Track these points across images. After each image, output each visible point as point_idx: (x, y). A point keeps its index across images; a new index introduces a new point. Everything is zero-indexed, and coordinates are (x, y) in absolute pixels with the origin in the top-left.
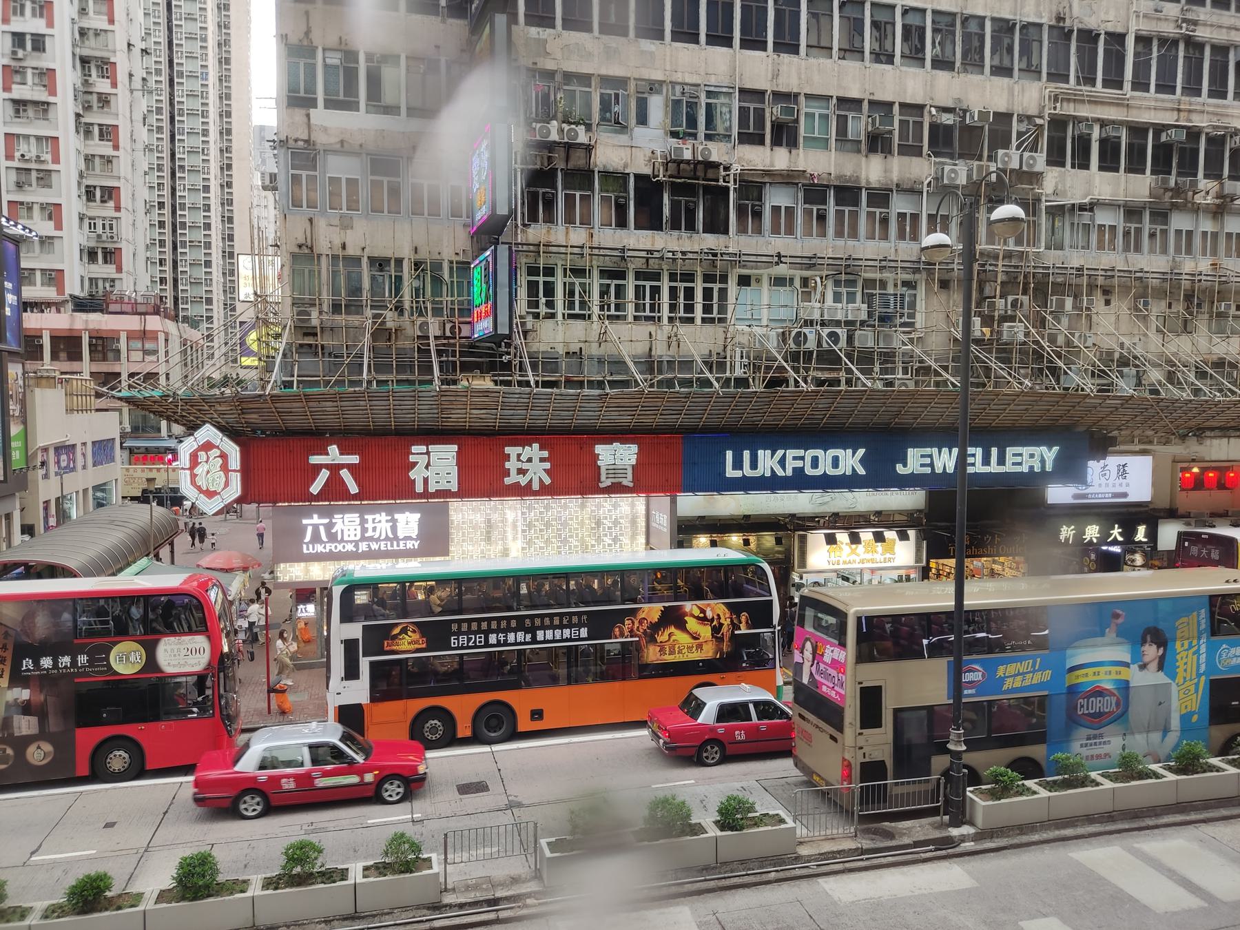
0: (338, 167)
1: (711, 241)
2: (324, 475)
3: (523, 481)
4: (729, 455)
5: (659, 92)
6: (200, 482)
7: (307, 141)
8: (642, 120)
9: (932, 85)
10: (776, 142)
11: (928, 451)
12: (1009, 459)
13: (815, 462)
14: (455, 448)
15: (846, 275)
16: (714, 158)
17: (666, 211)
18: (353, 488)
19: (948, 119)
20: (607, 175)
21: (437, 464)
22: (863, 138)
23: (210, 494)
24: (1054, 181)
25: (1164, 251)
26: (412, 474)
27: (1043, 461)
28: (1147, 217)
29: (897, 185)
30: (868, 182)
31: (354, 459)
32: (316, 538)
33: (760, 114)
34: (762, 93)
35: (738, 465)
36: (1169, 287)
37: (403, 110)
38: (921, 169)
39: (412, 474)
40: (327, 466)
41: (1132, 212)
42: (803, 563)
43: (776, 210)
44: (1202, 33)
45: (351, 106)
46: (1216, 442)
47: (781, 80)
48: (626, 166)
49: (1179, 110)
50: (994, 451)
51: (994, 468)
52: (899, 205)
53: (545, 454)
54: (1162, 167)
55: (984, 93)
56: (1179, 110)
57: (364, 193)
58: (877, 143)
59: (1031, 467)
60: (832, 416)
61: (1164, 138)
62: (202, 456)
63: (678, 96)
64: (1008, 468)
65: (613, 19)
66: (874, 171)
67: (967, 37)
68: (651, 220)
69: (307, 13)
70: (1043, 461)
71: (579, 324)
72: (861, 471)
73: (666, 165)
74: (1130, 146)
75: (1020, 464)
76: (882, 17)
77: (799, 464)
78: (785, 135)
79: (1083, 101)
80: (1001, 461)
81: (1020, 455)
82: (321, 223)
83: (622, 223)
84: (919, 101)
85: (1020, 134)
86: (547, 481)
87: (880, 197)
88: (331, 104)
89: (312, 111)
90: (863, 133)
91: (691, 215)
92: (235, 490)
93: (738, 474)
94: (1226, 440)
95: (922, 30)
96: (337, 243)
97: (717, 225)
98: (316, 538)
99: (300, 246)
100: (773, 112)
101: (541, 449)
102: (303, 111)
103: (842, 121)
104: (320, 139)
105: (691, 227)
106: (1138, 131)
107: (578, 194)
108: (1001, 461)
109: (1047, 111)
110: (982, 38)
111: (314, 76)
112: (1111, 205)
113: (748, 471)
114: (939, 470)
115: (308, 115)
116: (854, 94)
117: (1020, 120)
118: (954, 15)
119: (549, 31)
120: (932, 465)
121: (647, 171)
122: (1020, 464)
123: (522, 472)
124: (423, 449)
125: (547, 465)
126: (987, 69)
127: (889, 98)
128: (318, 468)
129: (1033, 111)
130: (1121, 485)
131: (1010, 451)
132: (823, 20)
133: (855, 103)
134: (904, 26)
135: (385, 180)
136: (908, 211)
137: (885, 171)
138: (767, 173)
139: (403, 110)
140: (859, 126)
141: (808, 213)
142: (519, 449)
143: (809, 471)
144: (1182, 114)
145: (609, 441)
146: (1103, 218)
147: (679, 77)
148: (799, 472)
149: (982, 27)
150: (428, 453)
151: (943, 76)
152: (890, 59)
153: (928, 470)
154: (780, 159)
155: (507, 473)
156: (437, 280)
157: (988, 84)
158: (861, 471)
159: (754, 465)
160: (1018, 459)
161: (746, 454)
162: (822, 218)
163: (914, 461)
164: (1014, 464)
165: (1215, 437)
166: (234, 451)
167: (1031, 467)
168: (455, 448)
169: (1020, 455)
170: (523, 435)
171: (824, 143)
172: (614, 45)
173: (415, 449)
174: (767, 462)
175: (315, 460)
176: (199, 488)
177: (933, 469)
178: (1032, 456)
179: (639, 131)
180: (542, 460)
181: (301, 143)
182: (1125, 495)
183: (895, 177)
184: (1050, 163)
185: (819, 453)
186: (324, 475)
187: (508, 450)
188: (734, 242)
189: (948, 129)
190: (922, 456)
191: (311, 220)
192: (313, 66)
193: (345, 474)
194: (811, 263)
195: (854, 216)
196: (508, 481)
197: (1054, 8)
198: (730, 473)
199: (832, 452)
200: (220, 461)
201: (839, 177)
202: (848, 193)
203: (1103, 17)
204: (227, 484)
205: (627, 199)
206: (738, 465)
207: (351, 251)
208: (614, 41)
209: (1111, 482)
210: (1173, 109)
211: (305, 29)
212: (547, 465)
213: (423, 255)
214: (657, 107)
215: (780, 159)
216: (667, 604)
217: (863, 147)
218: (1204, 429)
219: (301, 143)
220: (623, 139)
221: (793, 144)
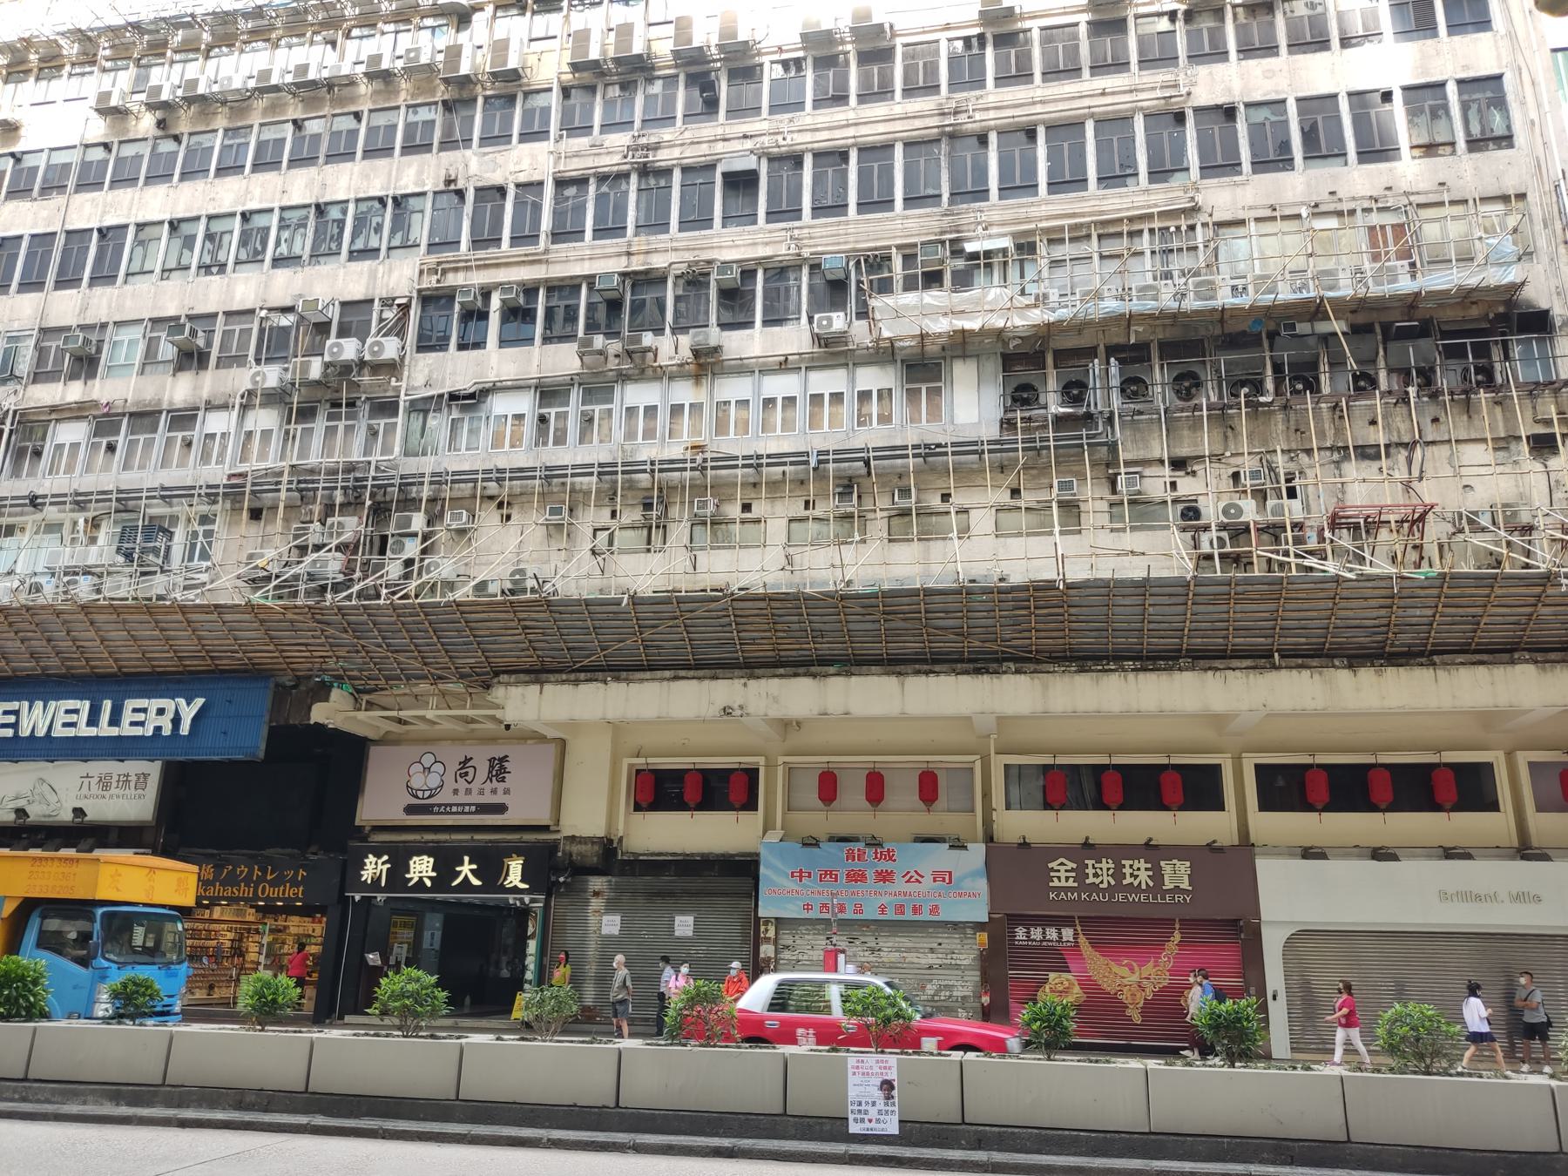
9: (266, 286)
10: (73, 376)
11: (14, 705)
12: (128, 716)
19: (286, 321)
24: (426, 371)
27: (176, 721)
28: (575, 395)
29: (208, 402)
30: (171, 403)
36: (615, 483)
41: (549, 392)
44: (664, 157)
46: (515, 692)
47: (89, 313)
49: (629, 254)
50: (107, 705)
55: (336, 281)
56: (629, 254)
58: (191, 359)
59: (158, 729)
66: (181, 390)
70: (176, 721)
75: (141, 724)
79: (468, 268)
80: (115, 721)
81: (144, 710)
84: (248, 306)
94: (538, 687)
108: (115, 721)
112: (517, 387)
114: (25, 732)
120: (15, 726)
122: (141, 724)
127: (210, 309)
130: (494, 791)
131: (130, 704)
137: (195, 389)
138: (54, 409)
144: (634, 259)
151: (282, 275)
153: (9, 733)
154: (74, 392)
157: (342, 271)
160: (140, 717)
162: (111, 448)
164: (133, 724)
165: (517, 684)
167: (158, 729)
169: (144, 710)
177: (16, 732)
178: (161, 712)
182: (500, 809)
190: (6, 713)
197: (443, 173)
201: (137, 403)
203: (512, 168)
209: (475, 786)
210: (619, 255)
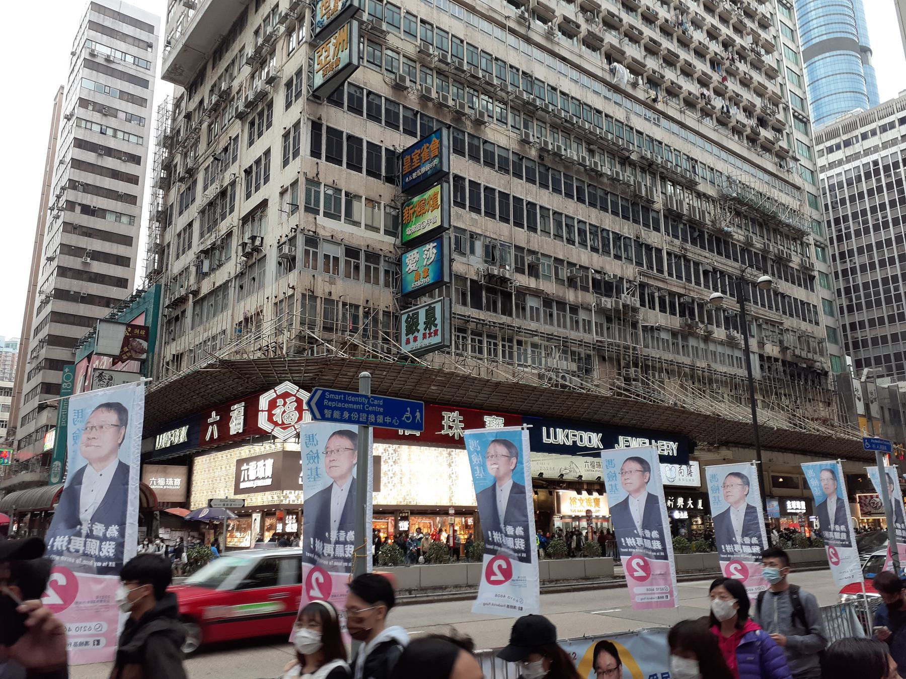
0: (326, 248)
1: (505, 319)
4: (544, 429)
5: (480, 240)
6: (278, 419)
7: (315, 232)
8: (472, 252)
15: (565, 346)
16: (507, 276)
17: (484, 300)
19: (598, 276)
25: (689, 356)
33: (523, 259)
34: (523, 249)
35: (548, 436)
37: (363, 225)
38: (590, 298)
42: (559, 511)
43: (531, 308)
45: (338, 218)
52: (582, 315)
53: (461, 418)
54: (682, 315)
55: (614, 268)
58: (571, 282)
60: (589, 413)
61: (682, 300)
63: (487, 243)
65: (459, 200)
66: (571, 296)
67: (603, 237)
68: (477, 304)
74: (670, 302)
76: (570, 222)
78: (533, 271)
82: (319, 279)
84: (587, 265)
85: (627, 289)
87: (574, 309)
88: (326, 215)
91: (495, 303)
95: (585, 232)
96: (327, 291)
97: (507, 311)
100: (528, 259)
102: (313, 216)
103: (556, 269)
104: (322, 233)
105: (495, 311)
106: (672, 294)
109: (638, 279)
110: (609, 239)
111: (319, 198)
113: (552, 440)
116: (561, 257)
118: (597, 227)
121: (475, 278)
123: (450, 427)
126: (612, 255)
129: (631, 279)
132: (546, 219)
133: (562, 261)
134: (579, 229)
135: (353, 260)
136: (587, 319)
140: (565, 273)
141: (545, 312)
145: (490, 415)
146: (664, 335)
147: (488, 234)
149: (608, 235)
152: (573, 243)
155: (442, 428)
156: (375, 320)
159: (556, 438)
161: (552, 430)
162: (551, 315)
170: (451, 406)
171: (548, 278)
174: (562, 436)
179: (472, 257)
180: (460, 422)
181: (311, 233)
184: (641, 305)
187: (444, 413)
188: (516, 322)
189: (599, 281)
192: (319, 192)
194: (550, 338)
195: (564, 317)
198: (545, 440)
202: (561, 305)
204: (300, 418)
205: (466, 290)
206: (548, 436)
207: (334, 297)
213: (371, 305)
214: (479, 245)
215: (532, 283)
216: (343, 621)
217: (566, 283)
219: (311, 233)
220: (464, 260)
221: (537, 277)
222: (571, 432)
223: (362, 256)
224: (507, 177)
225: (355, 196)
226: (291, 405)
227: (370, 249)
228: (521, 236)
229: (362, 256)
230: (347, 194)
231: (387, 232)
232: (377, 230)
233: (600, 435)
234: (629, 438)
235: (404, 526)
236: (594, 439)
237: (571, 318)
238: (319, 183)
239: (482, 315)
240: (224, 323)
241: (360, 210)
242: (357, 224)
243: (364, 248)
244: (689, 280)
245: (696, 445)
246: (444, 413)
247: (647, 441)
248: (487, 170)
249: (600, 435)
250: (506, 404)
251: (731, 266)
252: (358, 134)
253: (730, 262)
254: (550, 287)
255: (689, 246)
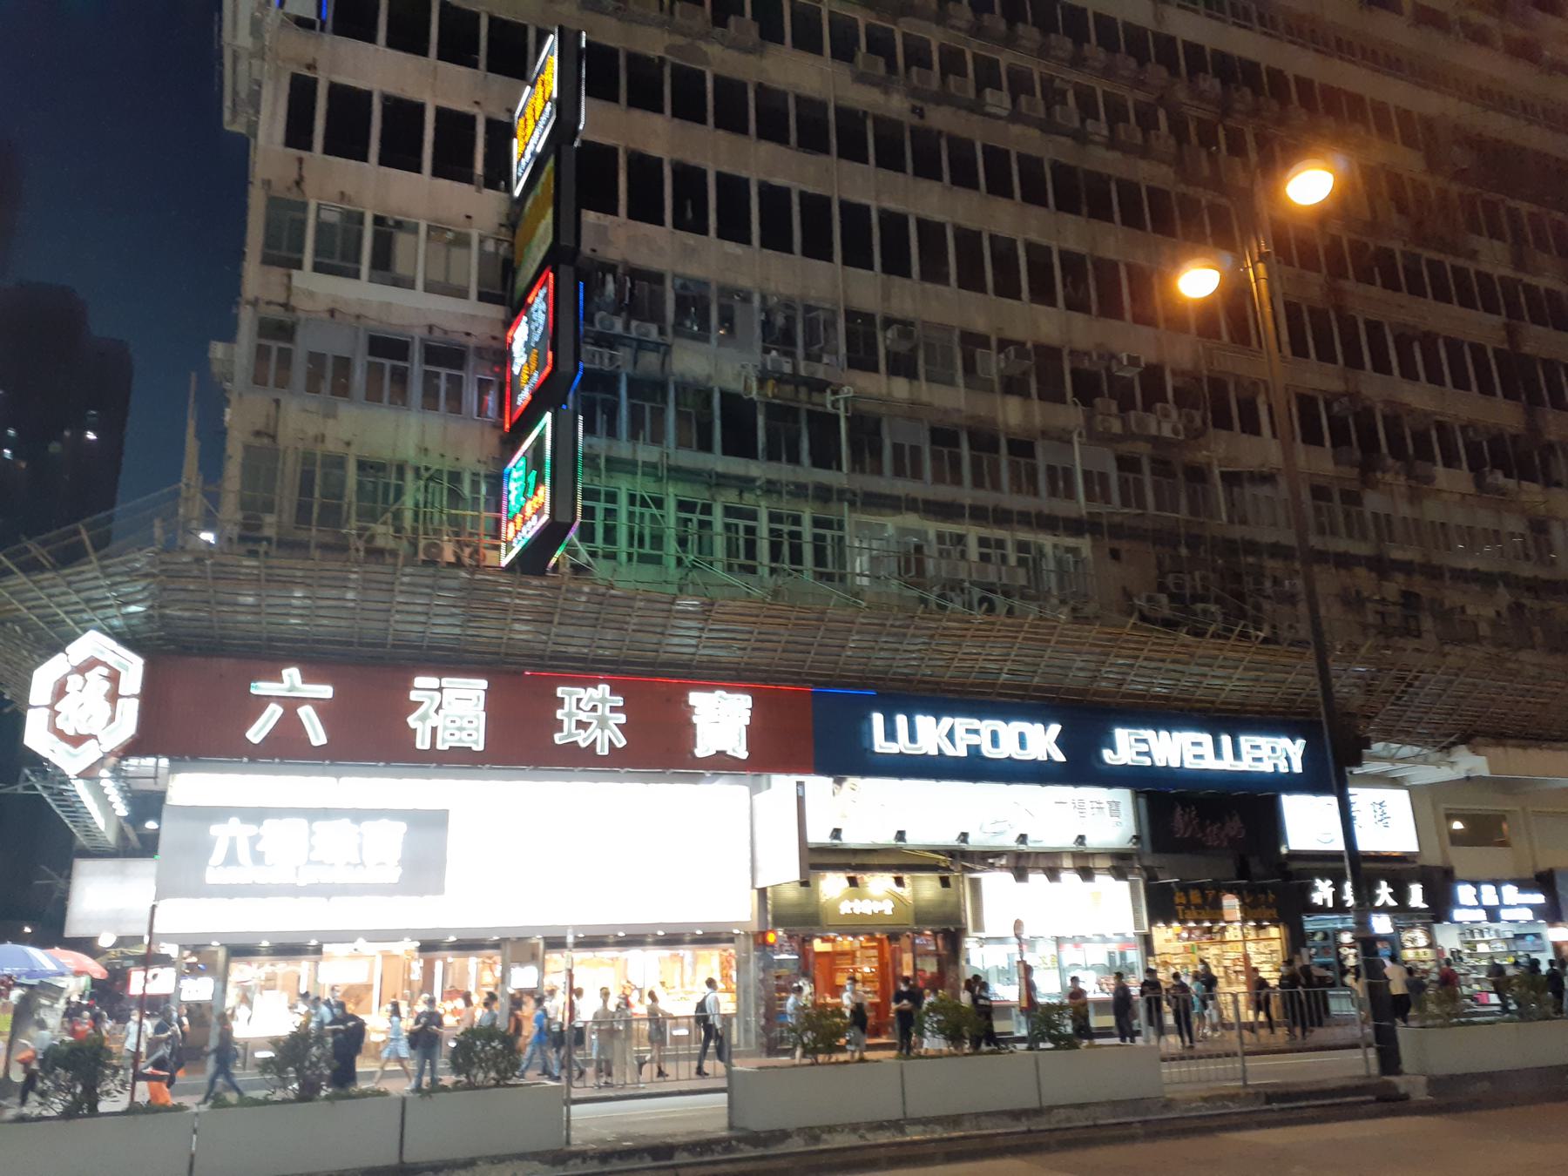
2: (273, 713)
3: (583, 739)
7: (286, 306)
13: (995, 742)
14: (483, 684)
18: (317, 735)
20: (683, 387)
21: (452, 708)
22: (996, 378)
23: (77, 740)
26: (412, 721)
31: (325, 691)
32: (231, 859)
35: (891, 735)
37: (420, 283)
39: (412, 721)
40: (279, 699)
42: (978, 926)
48: (709, 377)
51: (1227, 763)
53: (619, 701)
57: (359, 377)
61: (1336, 407)
62: (74, 682)
64: (1245, 765)
66: (1012, 413)
69: (301, 161)
71: (649, 572)
72: (1059, 757)
73: (762, 382)
77: (974, 740)
83: (705, 445)
86: (621, 742)
87: (1022, 448)
88: (318, 268)
89: (295, 272)
90: (994, 371)
92: (127, 722)
93: (892, 748)
98: (231, 859)
99: (258, 434)
101: (612, 693)
107: (647, 406)
113: (902, 745)
115: (289, 277)
117: (1174, 373)
119: (610, 217)
120: (1148, 754)
121: (736, 386)
123: (581, 725)
124: (432, 682)
125: (622, 719)
128: (268, 699)
129: (1187, 364)
135: (388, 363)
139: (420, 283)
140: (993, 364)
142: (580, 692)
143: (988, 751)
145: (710, 688)
148: (974, 750)
150: (440, 689)
153: (1147, 762)
155: (559, 726)
158: (1059, 757)
159: (913, 738)
161: (901, 720)
162: (956, 463)
163: (1127, 746)
166: (133, 668)
168: (483, 684)
170: (585, 672)
172: (692, 242)
173: (419, 681)
174: (931, 734)
175: (260, 688)
176: (61, 735)
180: (614, 709)
183: (1038, 421)
185: (998, 725)
186: (273, 713)
187: (560, 692)
191: (277, 402)
193: (307, 714)
196: (558, 739)
198: (880, 744)
199: (1018, 726)
200: (107, 685)
202: (985, 440)
206: (891, 735)
208: (691, 239)
211: (295, 176)
212: (622, 719)
218: (1477, 733)
221: (911, 375)
222: (961, 723)
223: (416, 354)
224: (822, 159)
225: (399, 225)
226: (97, 682)
227: (437, 333)
228: (866, 289)
229: (416, 354)
230: (379, 220)
231: (483, 297)
232: (462, 293)
233: (1055, 729)
234: (1148, 734)
235: (523, 977)
236: (1041, 741)
237: (1014, 467)
238: (304, 206)
239: (756, 469)
240: (653, 621)
241: (412, 253)
242: (407, 283)
243: (419, 333)
244: (1354, 362)
245: (1367, 744)
246: (560, 692)
247: (1206, 738)
248: (767, 149)
249: (1055, 729)
250: (760, 658)
251: (1481, 327)
252: (411, 92)
253: (1478, 316)
254: (952, 399)
255: (1349, 285)
